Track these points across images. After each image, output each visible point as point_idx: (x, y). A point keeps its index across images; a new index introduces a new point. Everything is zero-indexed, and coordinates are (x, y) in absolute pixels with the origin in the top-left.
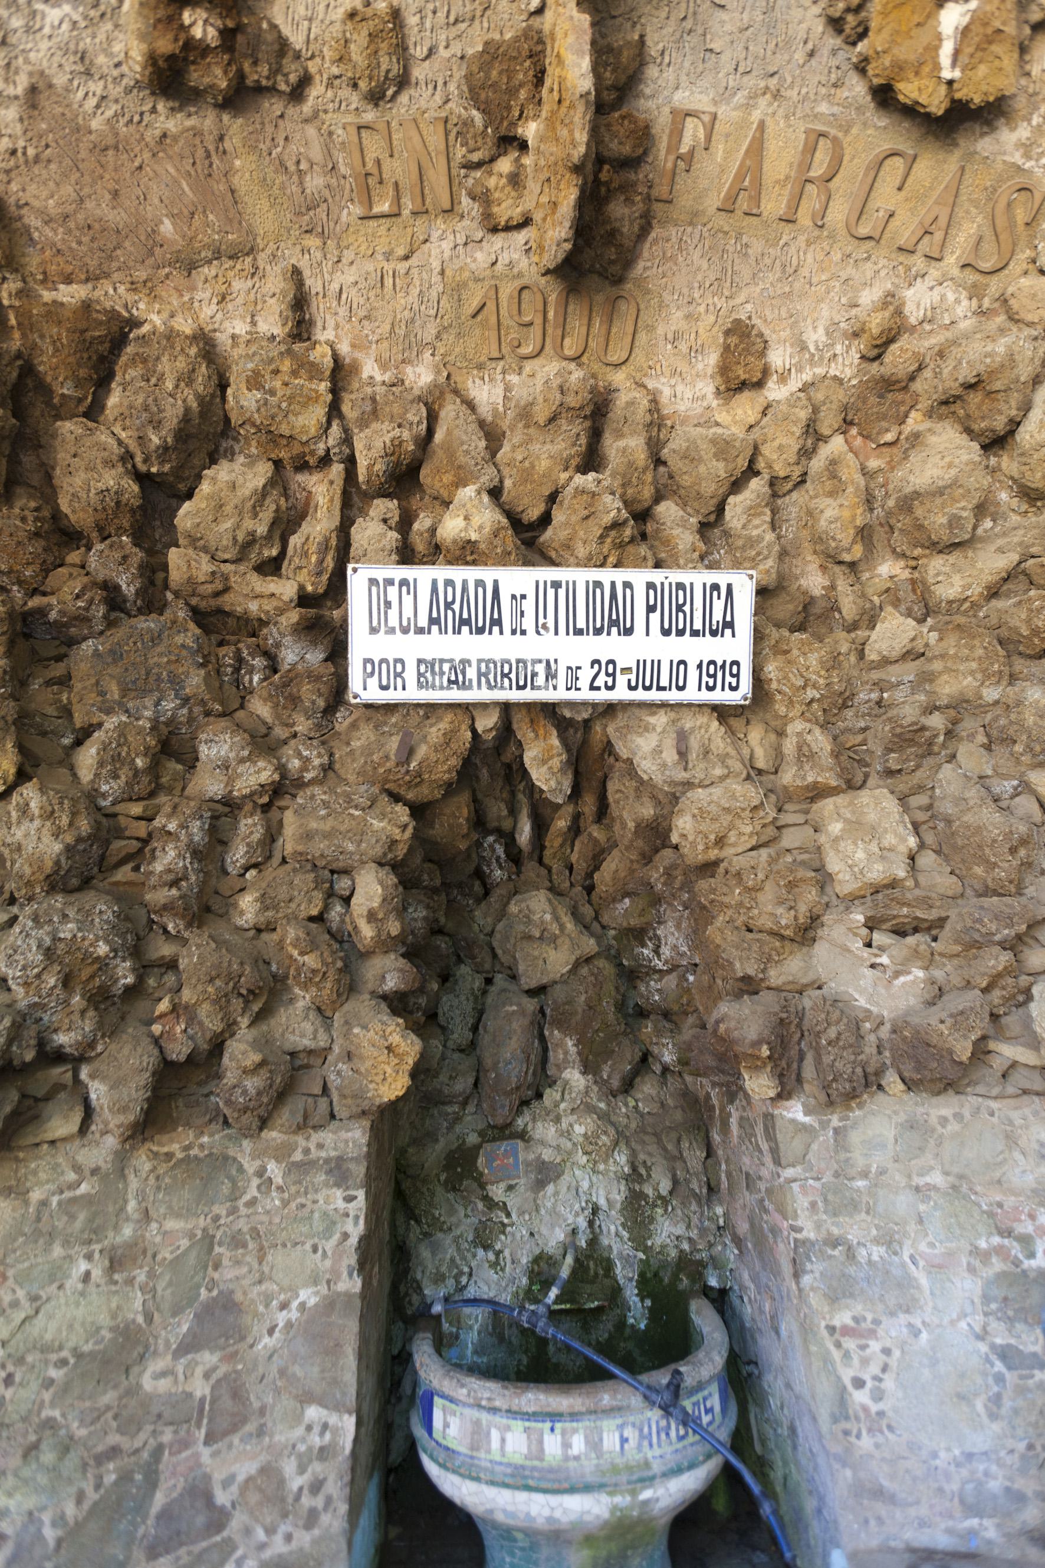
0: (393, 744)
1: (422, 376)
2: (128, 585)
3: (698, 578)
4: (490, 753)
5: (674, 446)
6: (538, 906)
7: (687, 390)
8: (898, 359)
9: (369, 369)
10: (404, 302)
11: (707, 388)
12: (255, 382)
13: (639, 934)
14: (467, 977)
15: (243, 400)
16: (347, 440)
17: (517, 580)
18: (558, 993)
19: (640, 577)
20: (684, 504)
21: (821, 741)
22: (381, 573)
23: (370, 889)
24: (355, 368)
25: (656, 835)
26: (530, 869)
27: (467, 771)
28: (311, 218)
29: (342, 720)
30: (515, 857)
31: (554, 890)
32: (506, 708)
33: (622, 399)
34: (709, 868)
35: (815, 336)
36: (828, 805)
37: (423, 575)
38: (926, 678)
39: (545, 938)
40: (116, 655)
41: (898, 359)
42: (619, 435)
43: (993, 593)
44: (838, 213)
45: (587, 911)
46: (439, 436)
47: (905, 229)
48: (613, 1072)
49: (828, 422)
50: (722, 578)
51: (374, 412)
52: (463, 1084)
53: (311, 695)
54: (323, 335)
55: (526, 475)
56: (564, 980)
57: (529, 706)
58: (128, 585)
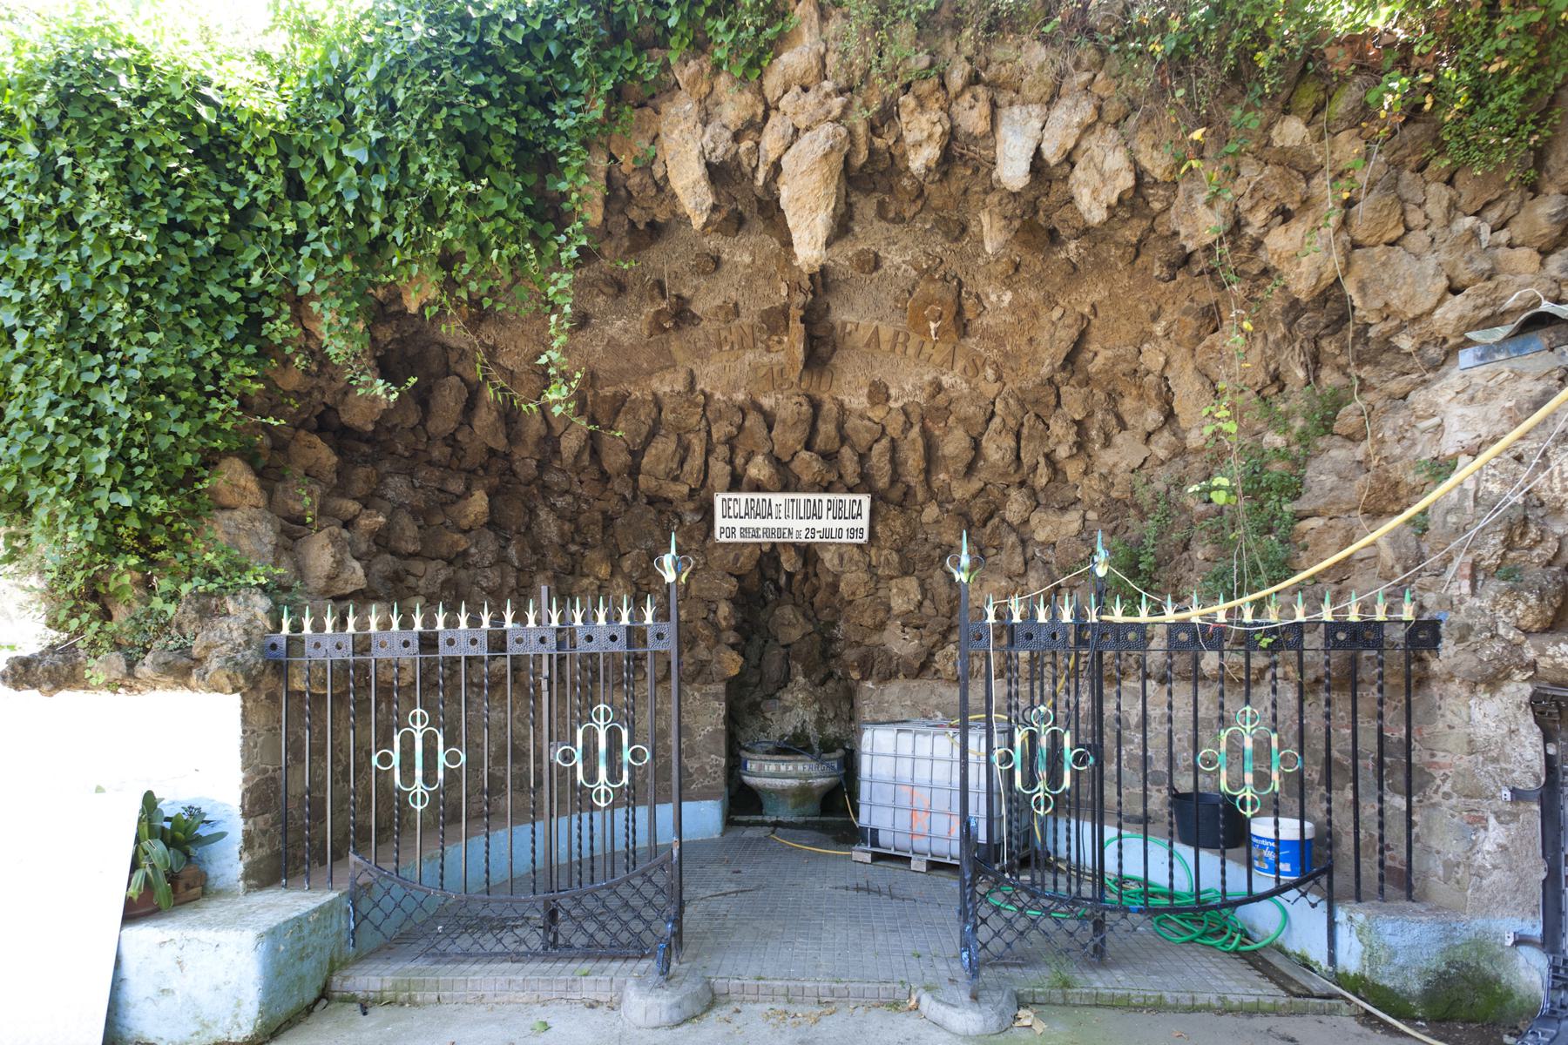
0: (731, 556)
1: (740, 397)
2: (629, 496)
3: (848, 498)
4: (769, 556)
5: (849, 425)
6: (788, 612)
7: (857, 401)
8: (941, 399)
9: (718, 395)
10: (732, 376)
11: (864, 400)
12: (674, 411)
13: (833, 624)
14: (757, 640)
15: (668, 416)
16: (709, 425)
17: (778, 499)
18: (796, 647)
19: (825, 497)
20: (852, 447)
21: (895, 557)
22: (727, 496)
23: (724, 609)
24: (712, 395)
25: (834, 587)
26: (785, 596)
27: (759, 562)
28: (701, 355)
29: (709, 543)
30: (778, 589)
31: (795, 605)
32: (774, 545)
33: (826, 407)
34: (850, 602)
35: (908, 387)
36: (893, 582)
37: (743, 497)
38: (939, 534)
39: (791, 625)
40: (630, 525)
41: (941, 399)
42: (825, 422)
43: (974, 497)
44: (911, 351)
45: (811, 613)
46: (747, 424)
47: (937, 358)
48: (816, 678)
49: (915, 418)
50: (857, 497)
51: (720, 415)
52: (755, 679)
53: (698, 535)
54: (698, 387)
55: (784, 446)
56: (798, 642)
57: (784, 544)
58: (629, 496)
